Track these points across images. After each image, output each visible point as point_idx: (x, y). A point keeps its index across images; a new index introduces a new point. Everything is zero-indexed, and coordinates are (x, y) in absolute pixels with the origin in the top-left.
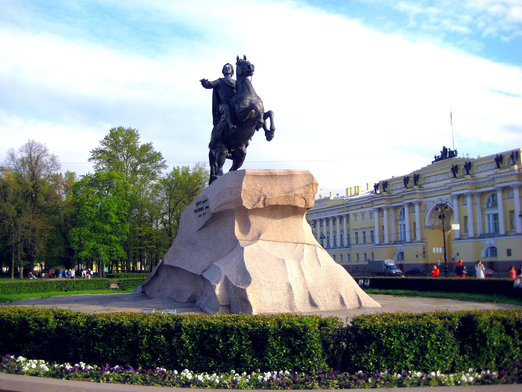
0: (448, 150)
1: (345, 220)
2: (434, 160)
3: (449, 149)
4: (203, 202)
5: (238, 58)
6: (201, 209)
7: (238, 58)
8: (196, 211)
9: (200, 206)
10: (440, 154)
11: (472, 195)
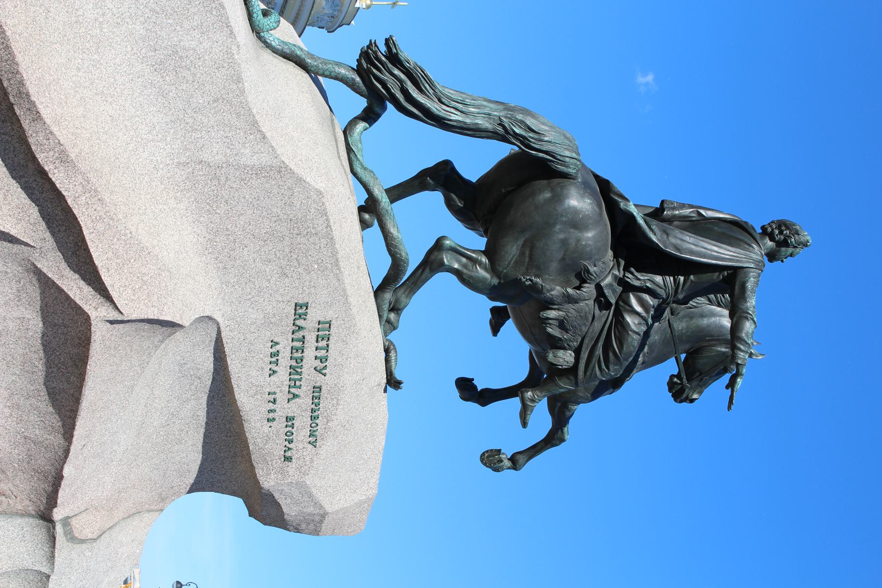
6: (295, 371)
8: (301, 309)
9: (310, 353)
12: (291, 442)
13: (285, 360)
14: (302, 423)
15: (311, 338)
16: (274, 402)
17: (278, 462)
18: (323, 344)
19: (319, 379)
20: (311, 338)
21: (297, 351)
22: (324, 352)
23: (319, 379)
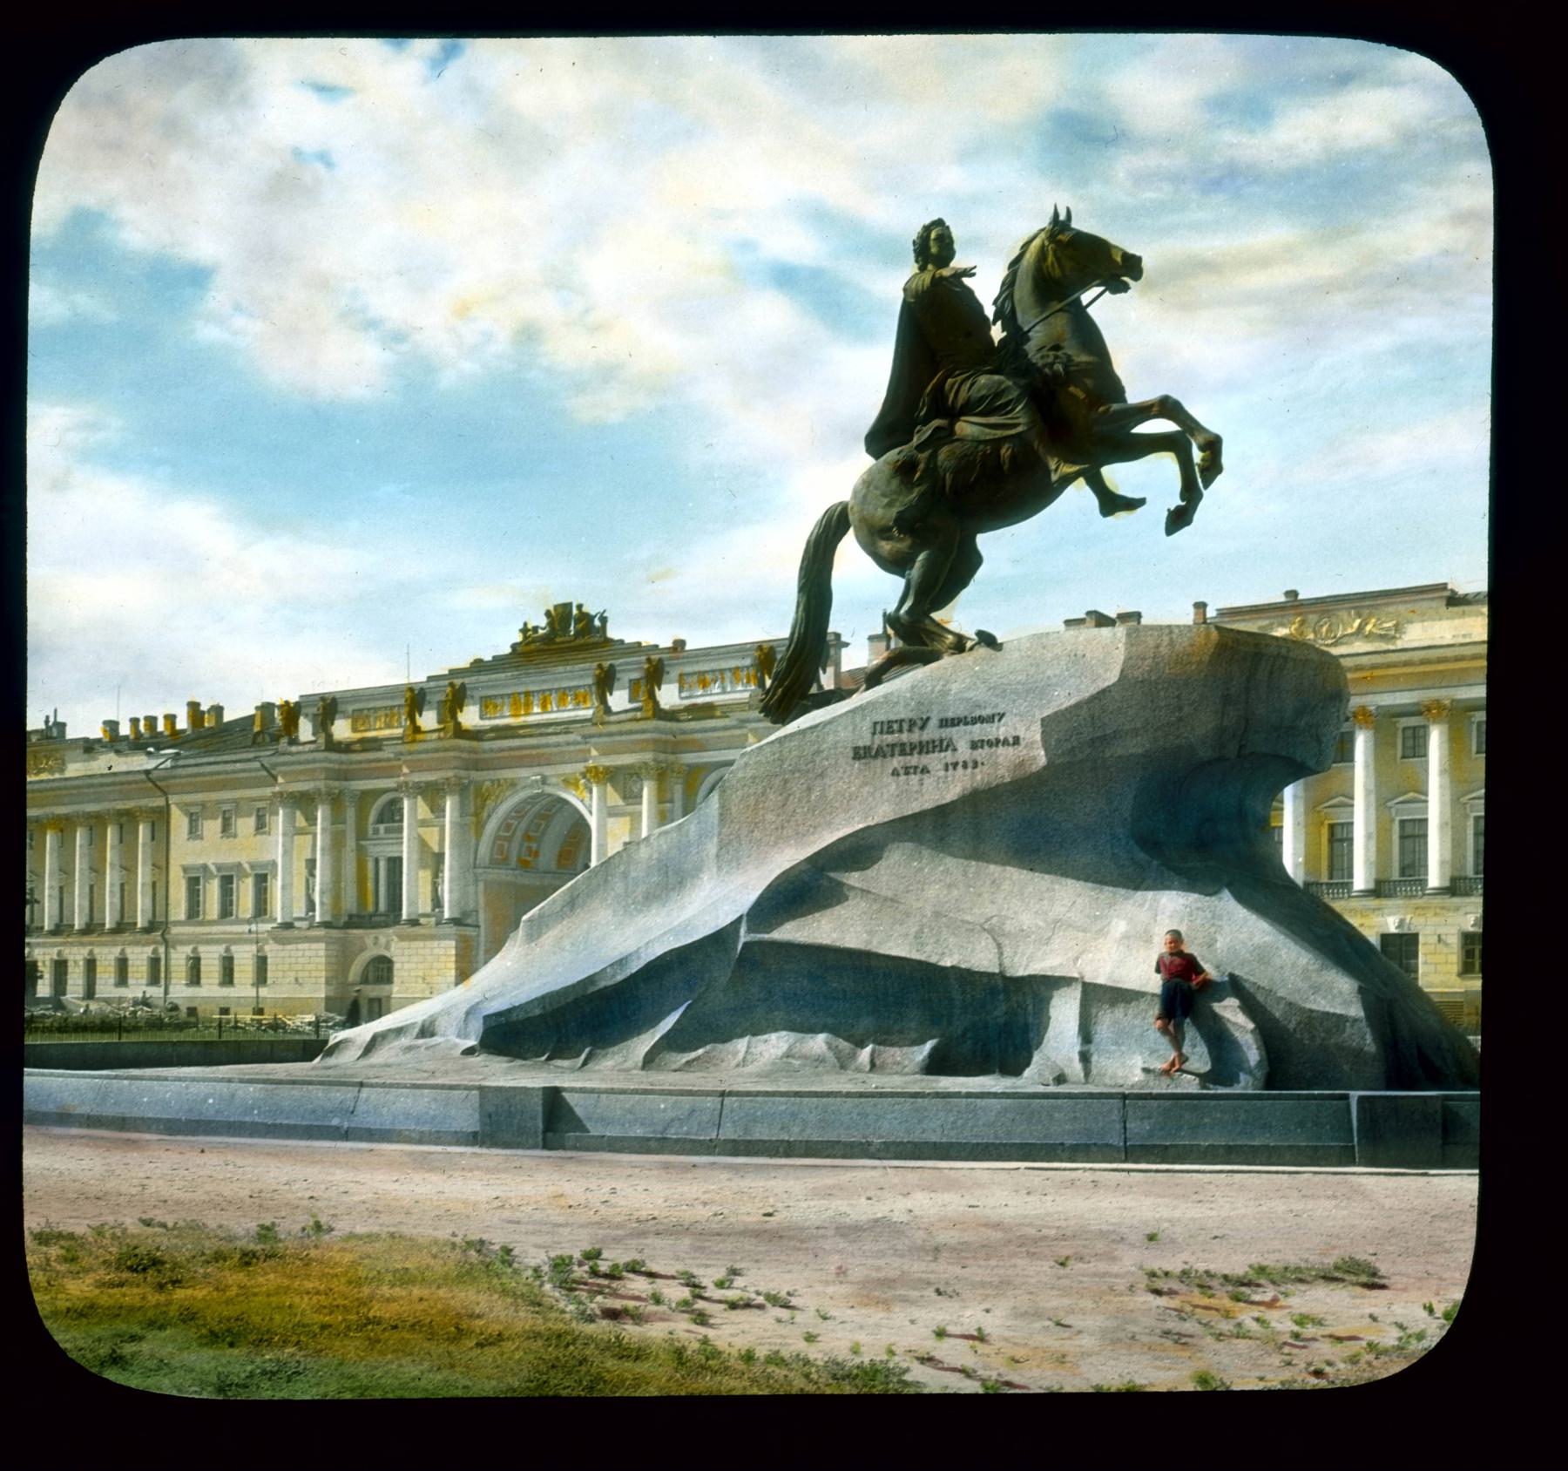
0: (575, 611)
1: (143, 831)
2: (518, 638)
3: (580, 607)
4: (945, 723)
5: (1056, 214)
6: (924, 748)
7: (1056, 214)
8: (860, 754)
9: (905, 737)
10: (542, 622)
11: (662, 775)
12: (998, 741)
13: (914, 760)
14: (977, 731)
15: (890, 738)
16: (955, 765)
17: (1021, 751)
18: (895, 727)
19: (934, 722)
20: (890, 738)
21: (904, 749)
22: (905, 726)
23: (934, 722)
